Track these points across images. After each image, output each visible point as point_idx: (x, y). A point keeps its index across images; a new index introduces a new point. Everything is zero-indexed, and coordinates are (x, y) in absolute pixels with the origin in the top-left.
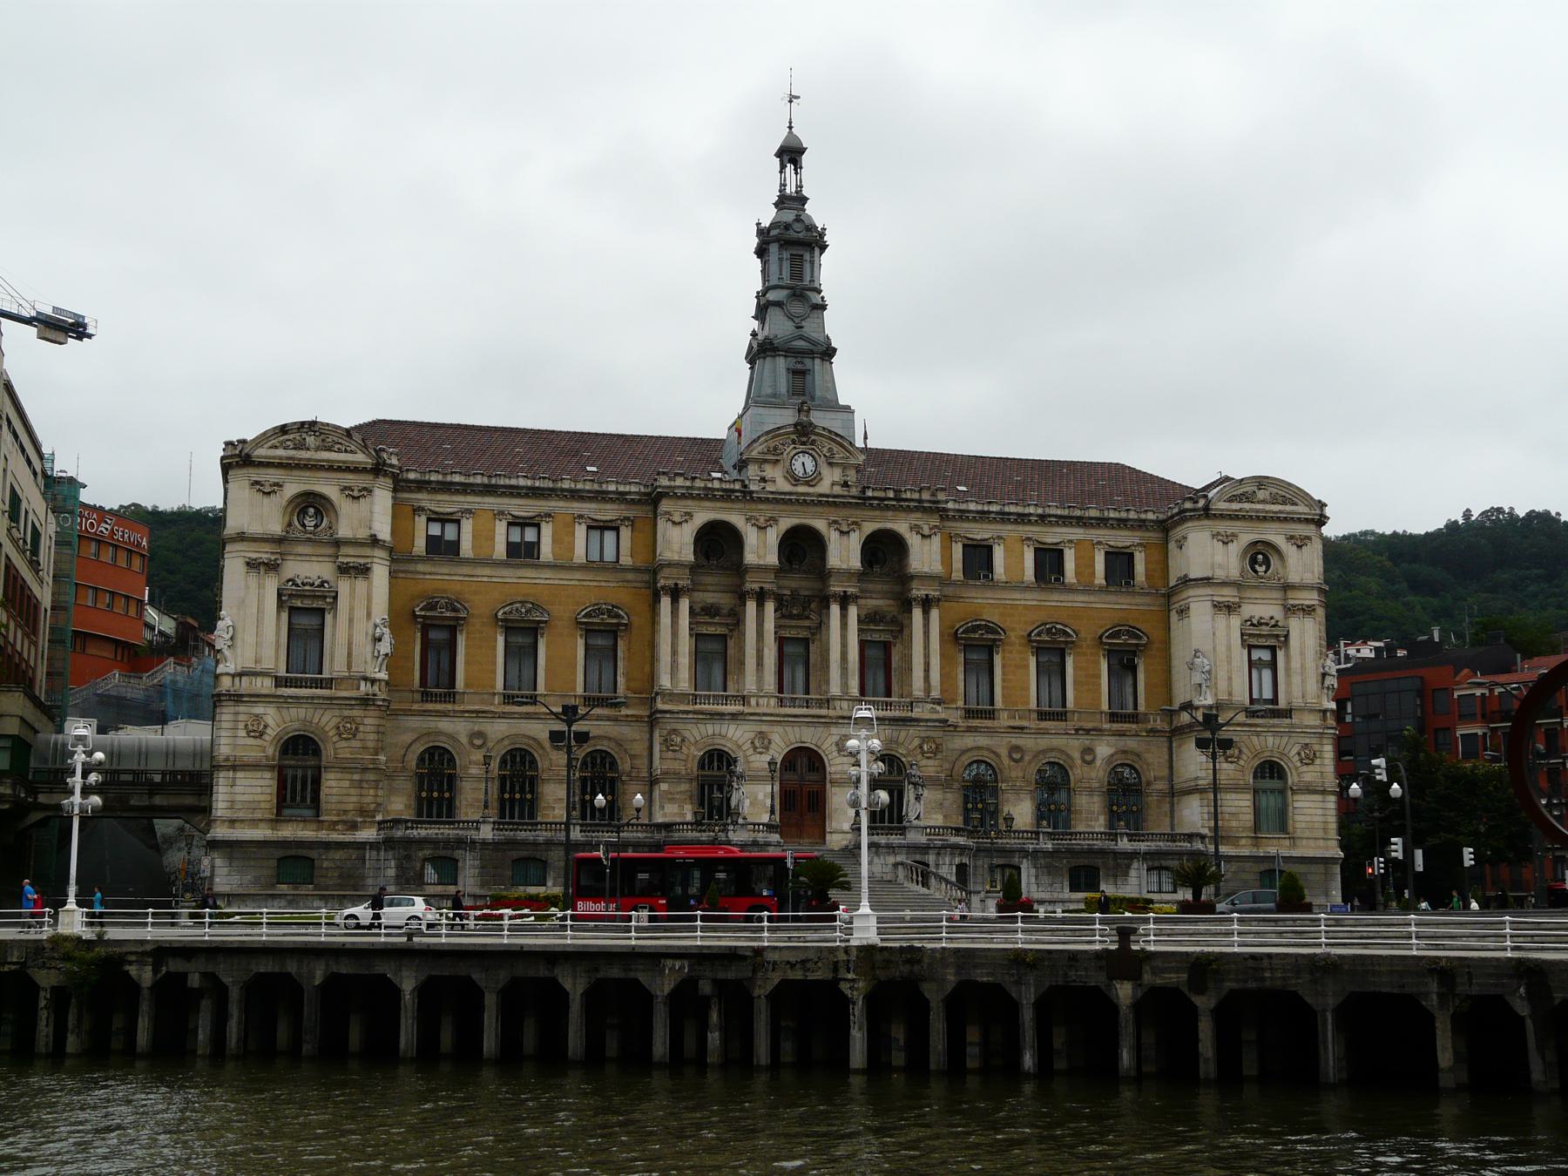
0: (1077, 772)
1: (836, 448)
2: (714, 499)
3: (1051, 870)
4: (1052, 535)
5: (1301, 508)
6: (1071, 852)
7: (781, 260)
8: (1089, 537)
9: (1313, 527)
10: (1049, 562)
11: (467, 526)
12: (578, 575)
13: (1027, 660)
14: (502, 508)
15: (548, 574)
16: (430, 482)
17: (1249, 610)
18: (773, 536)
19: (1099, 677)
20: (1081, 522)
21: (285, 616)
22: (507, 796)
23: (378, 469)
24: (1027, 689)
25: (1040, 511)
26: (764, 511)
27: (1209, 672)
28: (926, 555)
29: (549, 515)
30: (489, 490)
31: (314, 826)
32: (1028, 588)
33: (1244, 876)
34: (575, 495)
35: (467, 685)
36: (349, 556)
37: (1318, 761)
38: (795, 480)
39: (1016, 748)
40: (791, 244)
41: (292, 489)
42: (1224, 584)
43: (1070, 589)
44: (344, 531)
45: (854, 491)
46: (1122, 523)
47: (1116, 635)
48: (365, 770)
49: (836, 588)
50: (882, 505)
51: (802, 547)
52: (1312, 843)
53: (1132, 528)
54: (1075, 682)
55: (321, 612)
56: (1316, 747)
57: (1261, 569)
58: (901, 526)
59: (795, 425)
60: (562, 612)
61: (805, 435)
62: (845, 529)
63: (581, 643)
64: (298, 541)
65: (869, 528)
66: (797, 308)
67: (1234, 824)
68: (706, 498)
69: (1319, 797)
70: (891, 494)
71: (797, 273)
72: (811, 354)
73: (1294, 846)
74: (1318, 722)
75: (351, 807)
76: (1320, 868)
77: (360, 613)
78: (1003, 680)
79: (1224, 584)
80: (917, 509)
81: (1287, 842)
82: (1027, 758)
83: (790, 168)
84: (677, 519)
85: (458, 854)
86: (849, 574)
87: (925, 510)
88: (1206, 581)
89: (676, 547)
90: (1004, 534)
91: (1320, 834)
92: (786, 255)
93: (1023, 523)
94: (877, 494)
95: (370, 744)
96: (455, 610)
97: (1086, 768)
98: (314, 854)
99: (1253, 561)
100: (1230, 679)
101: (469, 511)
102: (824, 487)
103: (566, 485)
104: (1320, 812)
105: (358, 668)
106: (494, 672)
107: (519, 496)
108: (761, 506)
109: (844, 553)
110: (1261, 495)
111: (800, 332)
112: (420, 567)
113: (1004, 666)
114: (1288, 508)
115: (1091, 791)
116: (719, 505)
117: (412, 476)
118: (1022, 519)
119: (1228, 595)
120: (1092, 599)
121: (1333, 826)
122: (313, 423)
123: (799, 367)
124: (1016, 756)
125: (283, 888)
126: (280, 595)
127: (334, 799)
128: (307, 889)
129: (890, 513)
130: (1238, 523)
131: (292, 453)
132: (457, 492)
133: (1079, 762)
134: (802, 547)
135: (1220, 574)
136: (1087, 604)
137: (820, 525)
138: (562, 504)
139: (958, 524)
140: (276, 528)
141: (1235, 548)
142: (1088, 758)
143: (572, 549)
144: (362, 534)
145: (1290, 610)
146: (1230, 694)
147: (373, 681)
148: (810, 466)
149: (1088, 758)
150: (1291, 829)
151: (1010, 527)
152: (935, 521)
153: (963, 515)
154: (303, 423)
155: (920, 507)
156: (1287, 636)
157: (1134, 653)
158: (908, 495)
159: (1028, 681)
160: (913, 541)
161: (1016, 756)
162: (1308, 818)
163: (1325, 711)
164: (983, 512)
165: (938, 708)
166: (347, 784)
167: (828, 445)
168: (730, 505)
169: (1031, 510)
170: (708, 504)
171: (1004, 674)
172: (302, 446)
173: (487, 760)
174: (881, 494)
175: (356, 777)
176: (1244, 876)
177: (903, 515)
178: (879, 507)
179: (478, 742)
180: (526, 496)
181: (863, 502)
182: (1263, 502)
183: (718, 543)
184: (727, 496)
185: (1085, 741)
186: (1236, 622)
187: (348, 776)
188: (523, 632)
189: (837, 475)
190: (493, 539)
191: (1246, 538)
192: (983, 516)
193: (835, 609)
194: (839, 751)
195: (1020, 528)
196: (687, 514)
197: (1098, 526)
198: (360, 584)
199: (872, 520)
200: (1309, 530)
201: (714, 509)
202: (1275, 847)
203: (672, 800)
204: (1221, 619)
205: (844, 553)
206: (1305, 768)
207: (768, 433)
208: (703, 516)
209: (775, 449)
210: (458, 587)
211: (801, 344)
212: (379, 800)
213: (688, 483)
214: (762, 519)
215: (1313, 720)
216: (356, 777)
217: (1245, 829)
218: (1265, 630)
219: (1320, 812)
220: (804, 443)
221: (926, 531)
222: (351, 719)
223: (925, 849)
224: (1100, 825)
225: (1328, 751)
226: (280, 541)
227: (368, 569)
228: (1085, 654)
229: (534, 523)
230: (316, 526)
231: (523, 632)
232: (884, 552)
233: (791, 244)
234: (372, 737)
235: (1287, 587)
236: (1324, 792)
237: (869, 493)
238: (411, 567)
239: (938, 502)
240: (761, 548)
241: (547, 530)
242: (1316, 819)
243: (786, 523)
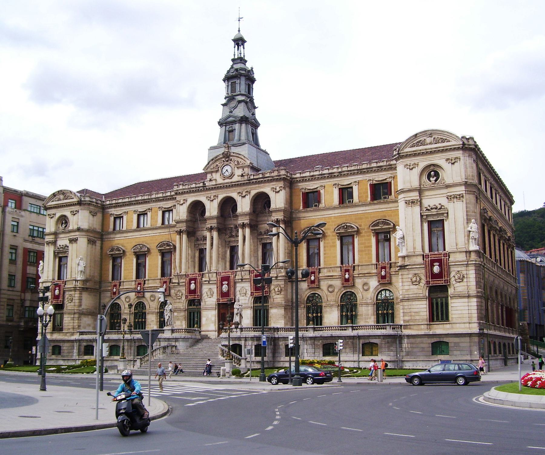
0: (359, 296)
1: (239, 160)
2: (193, 192)
3: (315, 346)
4: (345, 181)
5: (453, 143)
6: (322, 338)
7: (228, 86)
8: (364, 178)
9: (461, 152)
10: (345, 194)
11: (125, 218)
12: (159, 231)
13: (335, 242)
14: (136, 209)
15: (150, 232)
16: (112, 204)
17: (427, 202)
18: (216, 204)
19: (371, 246)
20: (361, 172)
21: (57, 260)
22: (344, 314)
23: (80, 203)
24: (336, 257)
25: (340, 170)
26: (212, 193)
27: (403, 238)
28: (278, 200)
29: (149, 209)
30: (130, 204)
31: (61, 334)
32: (335, 208)
33: (422, 345)
34: (158, 200)
35: (125, 279)
36: (73, 235)
37: (465, 280)
38: (225, 178)
39: (330, 286)
40: (240, 78)
41: (58, 215)
42: (410, 191)
43: (356, 206)
44: (71, 228)
45: (246, 178)
46: (380, 169)
47: (377, 225)
48: (74, 313)
49: (240, 221)
50: (258, 182)
51: (228, 206)
52: (462, 326)
53: (385, 170)
54: (359, 251)
55: (67, 256)
56: (464, 272)
57: (433, 179)
58: (267, 189)
59: (223, 153)
60: (153, 246)
61: (228, 157)
62: (244, 194)
63: (160, 258)
64: (60, 233)
65: (253, 192)
66: (233, 104)
67: (417, 318)
68: (190, 192)
69: (466, 300)
70: (261, 176)
71: (233, 90)
72: (234, 122)
73: (452, 328)
74: (465, 258)
75: (70, 327)
76: (467, 339)
77: (75, 256)
78: (325, 254)
79: (410, 191)
80: (272, 181)
81: (448, 326)
82: (336, 290)
83: (236, 46)
84: (182, 202)
85: (94, 344)
86: (244, 215)
87: (277, 180)
88: (403, 191)
89: (181, 214)
90: (323, 184)
91: (467, 320)
92: (230, 83)
93: (331, 177)
94: (255, 177)
95: (77, 304)
96: (119, 251)
97: (365, 293)
98: (61, 344)
99: (429, 176)
100: (414, 240)
101: (125, 212)
102: (235, 179)
103: (153, 196)
104: (467, 308)
105: (73, 276)
106: (132, 272)
107: (140, 204)
108: (212, 192)
109: (244, 205)
110: (428, 140)
111: (231, 114)
112: (112, 236)
113: (325, 247)
114: (446, 144)
115: (367, 304)
116: (196, 194)
117: (108, 203)
118: (331, 176)
119: (415, 195)
120: (367, 208)
121: (475, 316)
122: (61, 191)
123: (231, 129)
124: (330, 290)
125: (54, 357)
126: (54, 253)
127: (66, 325)
128: (59, 357)
129: (262, 185)
130: (418, 158)
131: (57, 203)
132: (121, 206)
133: (361, 290)
134: (228, 206)
135: (408, 186)
136: (364, 213)
137: (234, 195)
138: (154, 204)
139: (304, 184)
140: (53, 230)
141: (417, 171)
142: (365, 288)
143: (157, 221)
144: (75, 227)
145: (450, 198)
146: (414, 248)
147: (78, 281)
148: (230, 170)
149: (365, 288)
150: (450, 319)
151: (327, 181)
152: (281, 184)
153: (304, 180)
154: (59, 191)
155: (273, 180)
156: (447, 213)
157: (389, 232)
158: (268, 175)
159: (336, 253)
160: (272, 195)
161: (330, 290)
162: (460, 312)
163: (468, 252)
164: (313, 176)
165: (282, 270)
166: (70, 319)
167: (236, 159)
168: (200, 193)
169: (335, 170)
170: (192, 194)
171: (325, 250)
172: (59, 200)
173: (130, 306)
174: (257, 177)
175: (72, 316)
176: (422, 345)
177: (267, 184)
178: (256, 183)
179: (127, 300)
180: (142, 203)
181: (250, 182)
182: (430, 143)
183: (197, 209)
184: (197, 190)
185: (365, 280)
186: (417, 209)
187: (70, 316)
188: (141, 256)
189: (239, 172)
190: (132, 222)
191: (422, 165)
192: (313, 178)
193: (240, 231)
194: (240, 294)
195: (332, 180)
196: (184, 200)
197: (368, 172)
198: (75, 245)
199: (255, 189)
200: (459, 154)
201: (194, 196)
202: (440, 329)
203: (178, 319)
204: (410, 209)
205: (244, 205)
206: (458, 284)
207: (212, 160)
208: (191, 198)
209: (217, 165)
210: (122, 242)
211: (231, 119)
212: (79, 324)
213: (184, 187)
214: (212, 197)
215: (462, 257)
216: (72, 316)
217: (423, 320)
218: (434, 212)
219: (467, 308)
220: (227, 161)
221: (278, 189)
222: (71, 295)
223: (239, 339)
224: (372, 321)
225: (472, 273)
226: (56, 234)
227: (77, 240)
228: (362, 236)
229: (144, 214)
230: (66, 226)
231: (141, 256)
232: (261, 202)
233: (240, 78)
234: (77, 301)
235: (448, 186)
236: (469, 297)
237: (252, 177)
238: (109, 236)
239: (280, 176)
240: (212, 209)
241: (149, 214)
242: (464, 312)
243: (221, 197)
